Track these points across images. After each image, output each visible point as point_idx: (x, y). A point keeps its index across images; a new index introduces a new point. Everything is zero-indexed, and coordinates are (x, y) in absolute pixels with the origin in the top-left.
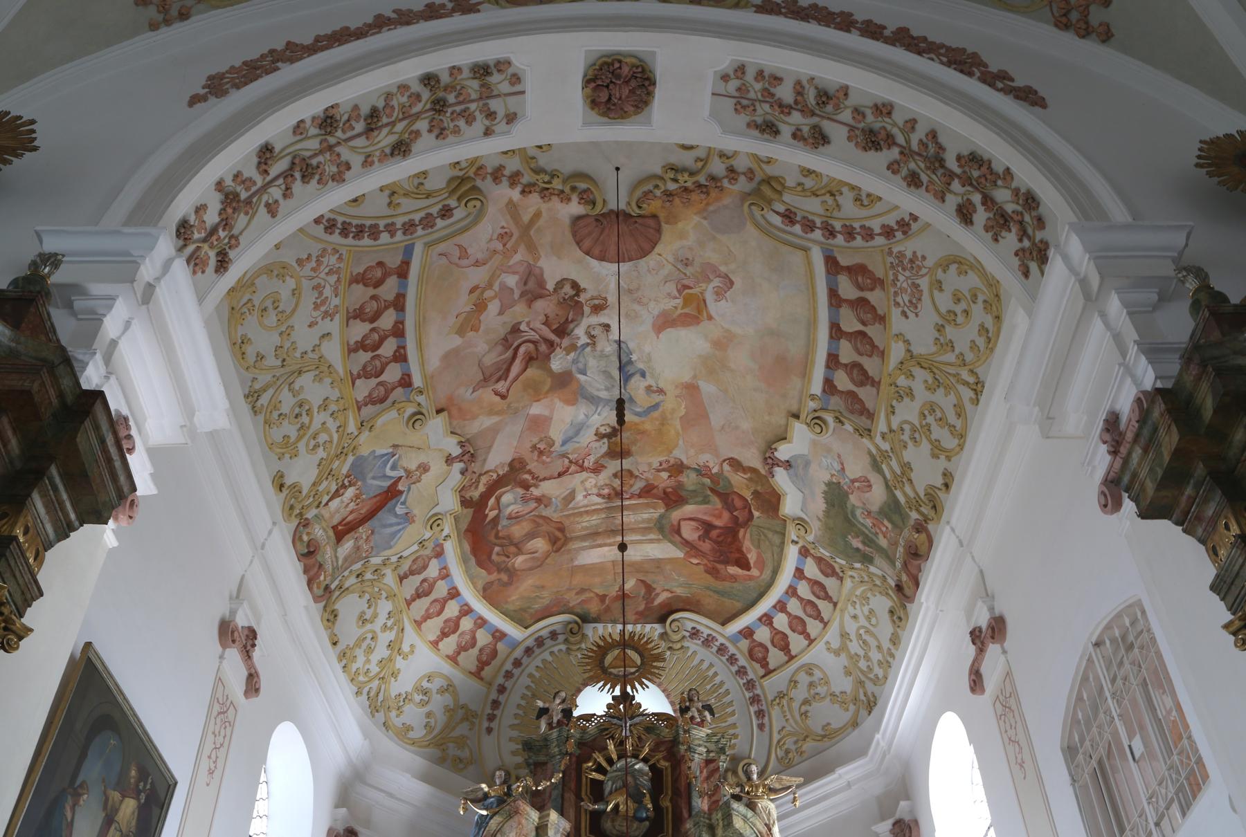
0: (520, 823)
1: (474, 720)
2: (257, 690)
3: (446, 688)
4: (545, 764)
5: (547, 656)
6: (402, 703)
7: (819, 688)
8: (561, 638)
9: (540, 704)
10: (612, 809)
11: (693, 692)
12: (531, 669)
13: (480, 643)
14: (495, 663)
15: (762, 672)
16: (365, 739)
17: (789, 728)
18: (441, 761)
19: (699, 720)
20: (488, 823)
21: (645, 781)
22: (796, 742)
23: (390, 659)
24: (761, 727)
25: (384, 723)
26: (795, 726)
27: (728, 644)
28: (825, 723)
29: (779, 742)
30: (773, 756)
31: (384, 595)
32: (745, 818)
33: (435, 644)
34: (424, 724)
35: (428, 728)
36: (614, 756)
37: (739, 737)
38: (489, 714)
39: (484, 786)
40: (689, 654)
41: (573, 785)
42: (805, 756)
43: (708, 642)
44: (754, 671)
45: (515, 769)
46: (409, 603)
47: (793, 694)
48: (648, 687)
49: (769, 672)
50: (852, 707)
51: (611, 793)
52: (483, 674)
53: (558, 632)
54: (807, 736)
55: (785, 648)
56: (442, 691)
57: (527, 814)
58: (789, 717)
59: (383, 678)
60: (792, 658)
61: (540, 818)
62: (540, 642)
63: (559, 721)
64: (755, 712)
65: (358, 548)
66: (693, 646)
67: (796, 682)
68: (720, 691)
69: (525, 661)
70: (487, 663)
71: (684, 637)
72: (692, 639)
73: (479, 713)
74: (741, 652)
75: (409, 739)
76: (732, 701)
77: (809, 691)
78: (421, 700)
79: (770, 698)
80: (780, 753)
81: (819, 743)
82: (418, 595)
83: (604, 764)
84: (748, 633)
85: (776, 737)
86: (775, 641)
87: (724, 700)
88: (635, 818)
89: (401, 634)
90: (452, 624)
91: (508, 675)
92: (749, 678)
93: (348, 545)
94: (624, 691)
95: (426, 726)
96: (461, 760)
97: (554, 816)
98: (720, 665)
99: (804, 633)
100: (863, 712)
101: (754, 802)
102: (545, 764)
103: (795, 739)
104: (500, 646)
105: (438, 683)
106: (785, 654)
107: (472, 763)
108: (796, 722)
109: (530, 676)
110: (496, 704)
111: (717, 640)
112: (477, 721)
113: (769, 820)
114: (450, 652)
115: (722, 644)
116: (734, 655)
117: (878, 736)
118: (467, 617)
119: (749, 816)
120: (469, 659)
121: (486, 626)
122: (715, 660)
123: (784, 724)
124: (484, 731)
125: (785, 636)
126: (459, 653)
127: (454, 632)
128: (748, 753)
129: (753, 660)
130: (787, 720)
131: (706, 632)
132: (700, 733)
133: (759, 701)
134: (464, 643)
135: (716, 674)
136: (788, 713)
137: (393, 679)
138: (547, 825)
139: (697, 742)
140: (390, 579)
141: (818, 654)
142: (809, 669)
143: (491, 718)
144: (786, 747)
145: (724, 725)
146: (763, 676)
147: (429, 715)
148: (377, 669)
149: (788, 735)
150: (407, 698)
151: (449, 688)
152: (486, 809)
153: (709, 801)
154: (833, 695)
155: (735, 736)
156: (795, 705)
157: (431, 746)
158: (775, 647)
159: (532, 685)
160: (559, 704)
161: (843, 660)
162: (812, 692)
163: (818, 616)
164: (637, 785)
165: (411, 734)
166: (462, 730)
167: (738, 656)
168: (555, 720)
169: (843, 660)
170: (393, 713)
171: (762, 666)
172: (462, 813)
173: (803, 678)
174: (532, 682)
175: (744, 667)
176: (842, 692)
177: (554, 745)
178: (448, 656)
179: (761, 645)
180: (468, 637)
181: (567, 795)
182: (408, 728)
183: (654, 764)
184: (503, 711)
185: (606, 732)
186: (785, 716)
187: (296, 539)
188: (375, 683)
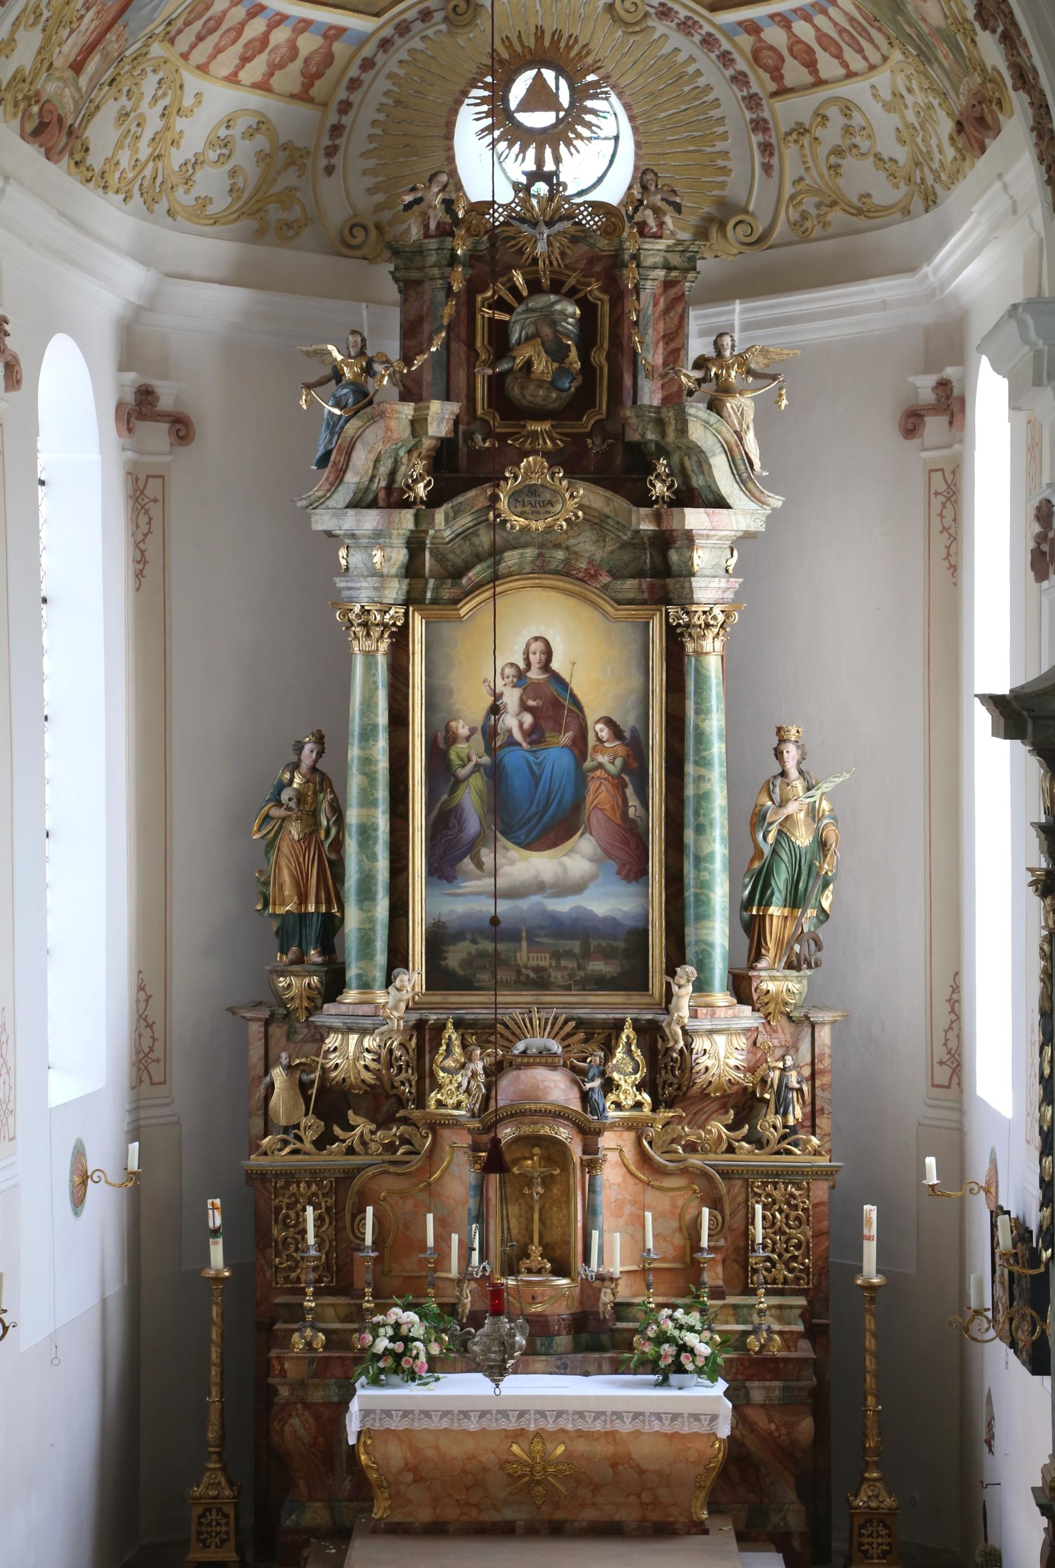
0: (388, 429)
1: (305, 161)
2: (18, 382)
3: (255, 126)
4: (419, 282)
5: (417, 43)
6: (191, 171)
7: (858, 138)
8: (438, 16)
9: (408, 198)
10: (521, 369)
11: (650, 176)
12: (392, 66)
13: (303, 53)
14: (331, 73)
15: (772, 87)
16: (148, 271)
17: (808, 181)
18: (258, 236)
19: (655, 230)
20: (342, 428)
21: (570, 325)
22: (818, 206)
23: (167, 128)
24: (767, 168)
25: (169, 211)
26: (818, 180)
27: (718, 36)
28: (863, 192)
29: (792, 197)
30: (782, 217)
31: (149, 69)
32: (706, 424)
33: (232, 79)
34: (229, 188)
35: (234, 194)
36: (525, 293)
37: (733, 174)
38: (327, 148)
39: (330, 347)
40: (656, 36)
41: (463, 332)
42: (830, 230)
43: (687, 27)
44: (760, 83)
45: (374, 212)
46: (185, 56)
47: (819, 132)
48: (578, 151)
49: (782, 91)
50: (903, 188)
51: (519, 342)
52: (313, 92)
53: (432, 9)
54: (834, 204)
55: (811, 65)
56: (250, 134)
57: (398, 412)
58: (810, 164)
59: (159, 157)
60: (819, 83)
61: (415, 410)
62: (403, 29)
63: (439, 224)
64: (760, 145)
65: (106, 56)
66: (661, 28)
67: (825, 118)
68: (705, 99)
69: (380, 58)
70: (319, 75)
71: (646, 15)
72: (661, 20)
73: (312, 149)
74: (741, 51)
75: (208, 217)
76: (724, 118)
77: (843, 136)
78: (219, 155)
79: (784, 128)
80: (794, 215)
81: (854, 218)
82: (200, 38)
83: (509, 298)
84: (752, 28)
85: (788, 190)
86: (795, 50)
87: (711, 113)
88: (553, 384)
89: (179, 92)
90: (257, 44)
91: (354, 84)
92: (752, 91)
93: (92, 65)
94: (540, 161)
95: (231, 191)
96: (289, 225)
97: (435, 406)
98: (706, 63)
99: (838, 56)
100: (918, 204)
101: (721, 400)
102: (419, 282)
103: (817, 199)
104: (337, 47)
105: (242, 124)
106: (810, 73)
107: (306, 225)
108: (821, 176)
109: (390, 76)
110: (337, 130)
111: (701, 27)
112: (308, 162)
113: (741, 424)
114: (257, 77)
115: (710, 35)
116: (729, 53)
117: (927, 269)
118: (281, 27)
119: (711, 422)
120: (289, 79)
121: (312, 28)
122: (698, 53)
123: (803, 173)
124: (321, 170)
125: (810, 51)
126: (271, 74)
127: (261, 51)
128: (744, 199)
129: (761, 67)
130: (807, 169)
131: (683, 13)
132: (655, 250)
133: (766, 130)
134: (278, 59)
135: (698, 73)
136: (809, 159)
137: (173, 150)
138: (426, 419)
139: (649, 262)
140: (157, 49)
141: (855, 90)
142: (847, 108)
143: (331, 151)
144: (803, 207)
145: (709, 149)
146: (775, 94)
147: (233, 173)
148: (150, 150)
149: (807, 191)
150: (197, 162)
151: (262, 125)
152: (337, 405)
153: (665, 349)
154: (878, 157)
155: (725, 171)
156: (823, 150)
157: (242, 217)
158: (795, 58)
159: (396, 89)
160: (439, 192)
161: (893, 120)
162: (848, 142)
163: (860, 51)
164: (556, 331)
165: (210, 210)
166: (288, 178)
167: (735, 55)
168: (433, 225)
169: (893, 120)
170: (181, 189)
171: (773, 79)
172: (304, 407)
173: (833, 112)
174: (394, 84)
175: (744, 74)
176: (891, 160)
177: (433, 258)
178: (255, 86)
179: (772, 48)
180: (284, 50)
181: (454, 346)
182: (204, 202)
183: (585, 296)
184: (349, 137)
185: (513, 243)
186: (804, 162)
187: (26, 116)
188: (148, 172)
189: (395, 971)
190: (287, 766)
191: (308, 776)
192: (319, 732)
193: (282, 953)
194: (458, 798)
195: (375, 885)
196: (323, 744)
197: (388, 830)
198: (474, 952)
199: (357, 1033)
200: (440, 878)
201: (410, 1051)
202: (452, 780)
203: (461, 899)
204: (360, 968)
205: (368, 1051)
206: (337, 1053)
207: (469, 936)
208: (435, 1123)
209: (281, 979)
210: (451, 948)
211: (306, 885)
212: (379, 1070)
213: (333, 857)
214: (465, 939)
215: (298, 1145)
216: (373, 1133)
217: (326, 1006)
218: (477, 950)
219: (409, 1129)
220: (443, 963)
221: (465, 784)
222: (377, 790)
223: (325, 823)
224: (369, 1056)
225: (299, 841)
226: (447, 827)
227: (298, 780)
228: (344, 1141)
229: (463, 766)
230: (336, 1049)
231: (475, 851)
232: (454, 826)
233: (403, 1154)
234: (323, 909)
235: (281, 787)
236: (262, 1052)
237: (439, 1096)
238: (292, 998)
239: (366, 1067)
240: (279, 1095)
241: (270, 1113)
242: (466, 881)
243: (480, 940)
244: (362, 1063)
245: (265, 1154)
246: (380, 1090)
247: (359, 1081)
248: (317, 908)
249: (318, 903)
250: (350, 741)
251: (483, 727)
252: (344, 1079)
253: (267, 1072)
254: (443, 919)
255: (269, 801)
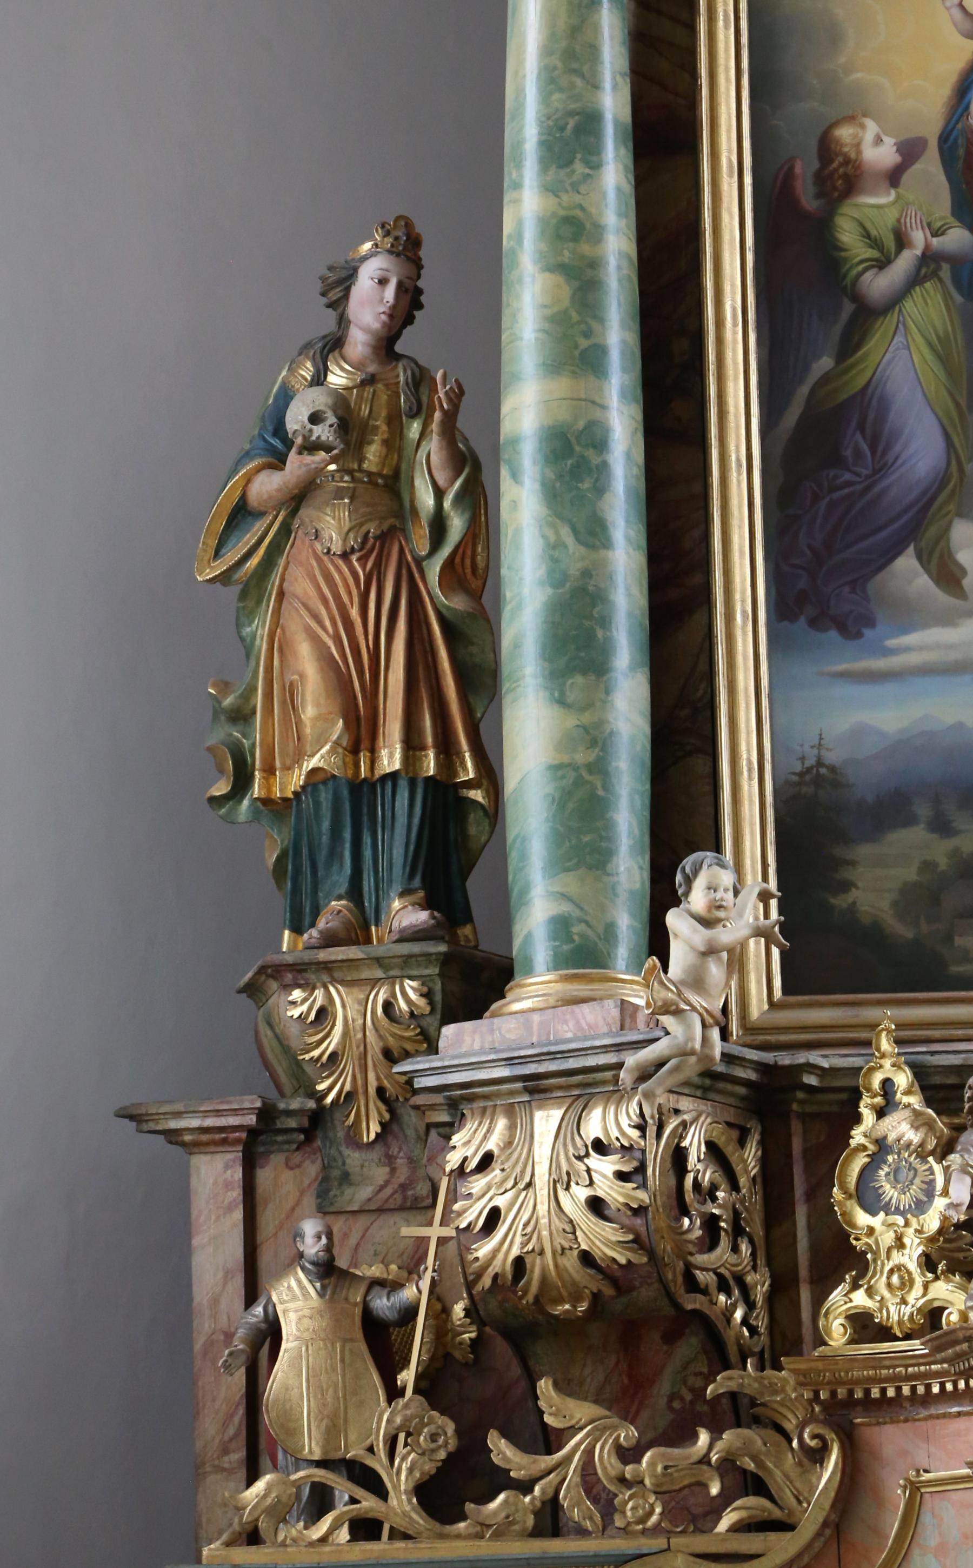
189: (688, 863)
190: (307, 346)
191: (372, 368)
192: (409, 225)
193: (297, 930)
194: (874, 359)
195: (605, 622)
196: (417, 264)
197: (639, 456)
198: (943, 863)
199: (558, 1101)
200: (816, 623)
201: (743, 1181)
202: (848, 308)
203: (888, 689)
204: (565, 897)
205: (600, 1147)
206: (495, 1174)
207: (923, 810)
208: (850, 1403)
209: (297, 994)
210: (864, 851)
211: (372, 693)
212: (639, 1211)
213: (457, 603)
214: (910, 821)
215: (369, 1503)
216: (629, 1455)
217: (449, 1031)
218: (955, 854)
219: (753, 1436)
220: (840, 901)
221: (892, 319)
222: (601, 320)
223: (426, 499)
224: (604, 1167)
225: (345, 556)
226: (835, 460)
227: (337, 378)
228: (525, 1487)
229: (882, 264)
230: (487, 1161)
231: (932, 532)
232: (858, 454)
233: (736, 1528)
234: (430, 765)
235: (286, 396)
236: (235, 1249)
237: (860, 1298)
238: (334, 1057)
239: (596, 1205)
240: (295, 1363)
241: (268, 1418)
242: (906, 630)
243: (959, 820)
244: (582, 1193)
245: (253, 1537)
246: (647, 1294)
247: (571, 1262)
248: (406, 759)
249: (412, 745)
250: (510, 173)
251: (944, 139)
252: (519, 1262)
253: (252, 1294)
254: (831, 757)
255: (247, 456)
